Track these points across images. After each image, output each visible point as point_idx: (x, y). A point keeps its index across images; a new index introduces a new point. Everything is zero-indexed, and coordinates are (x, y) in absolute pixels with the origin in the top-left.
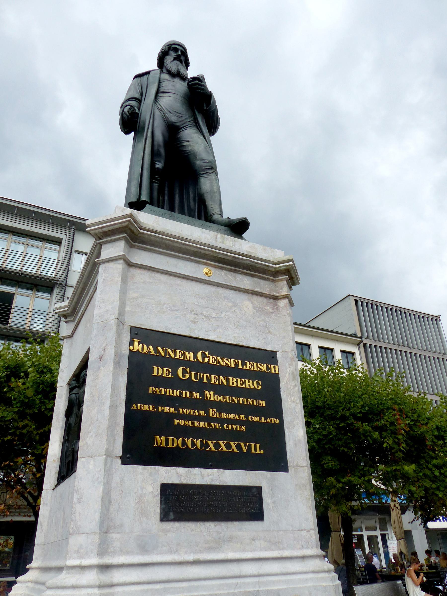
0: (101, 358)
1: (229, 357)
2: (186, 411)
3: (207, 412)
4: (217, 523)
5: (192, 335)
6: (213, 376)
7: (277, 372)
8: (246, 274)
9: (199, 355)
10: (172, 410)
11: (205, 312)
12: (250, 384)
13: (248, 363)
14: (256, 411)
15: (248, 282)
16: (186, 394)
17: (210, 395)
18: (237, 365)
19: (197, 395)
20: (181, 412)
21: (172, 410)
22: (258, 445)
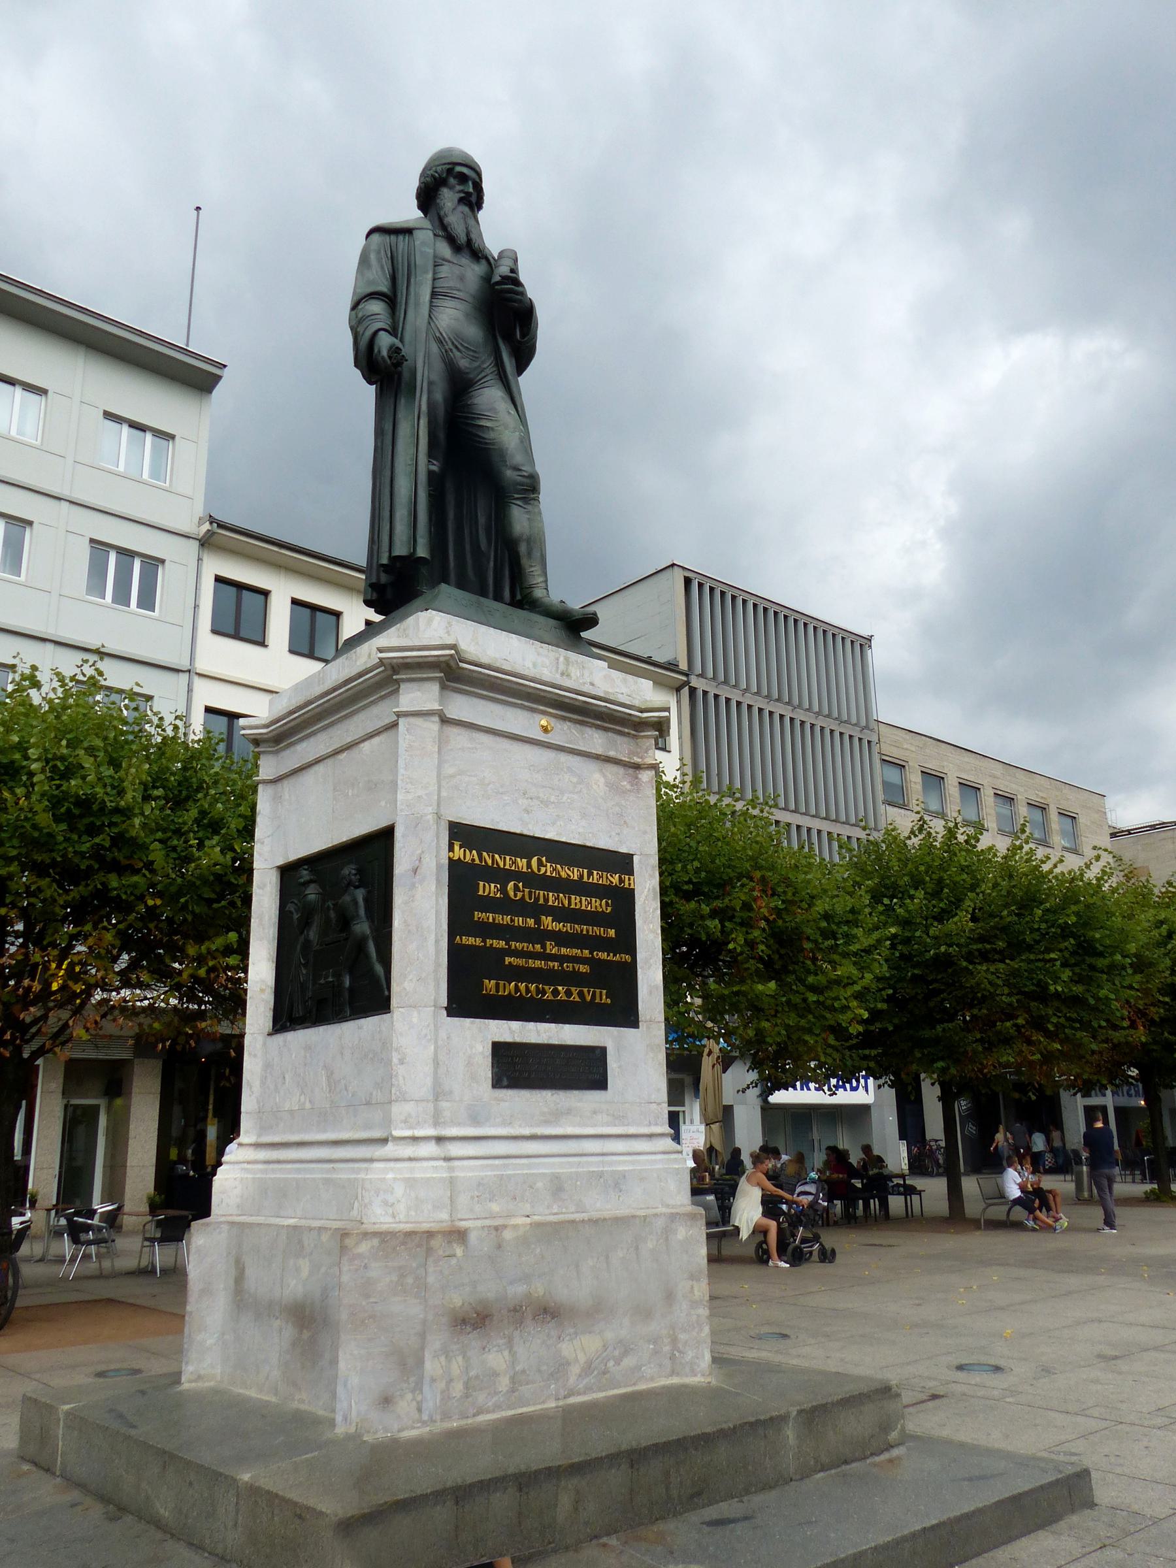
0: (415, 871)
1: (571, 864)
2: (519, 946)
3: (544, 947)
4: (554, 1092)
5: (526, 832)
6: (551, 894)
7: (632, 887)
8: (598, 727)
9: (534, 861)
10: (502, 944)
11: (541, 795)
13: (595, 872)
15: (600, 741)
16: (519, 921)
17: (548, 922)
18: (582, 876)
19: (531, 922)
20: (513, 947)
21: (502, 944)
22: (604, 991)
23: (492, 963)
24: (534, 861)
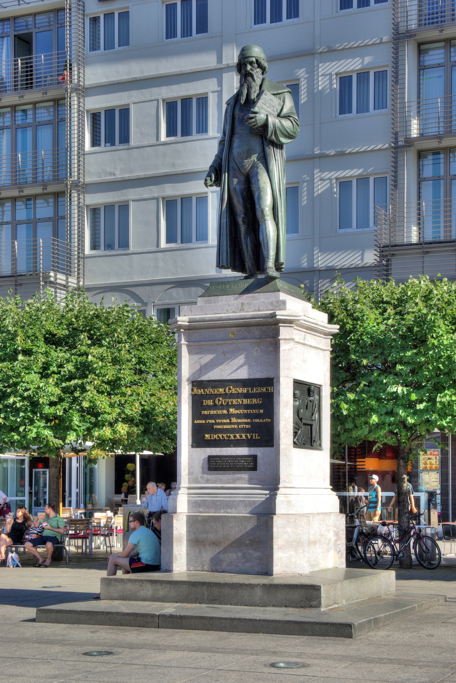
3: (230, 420)
6: (234, 400)
7: (272, 391)
9: (227, 389)
12: (255, 401)
13: (254, 388)
14: (258, 416)
16: (220, 412)
17: (232, 410)
21: (213, 421)
22: (257, 434)
23: (211, 429)
24: (227, 389)
